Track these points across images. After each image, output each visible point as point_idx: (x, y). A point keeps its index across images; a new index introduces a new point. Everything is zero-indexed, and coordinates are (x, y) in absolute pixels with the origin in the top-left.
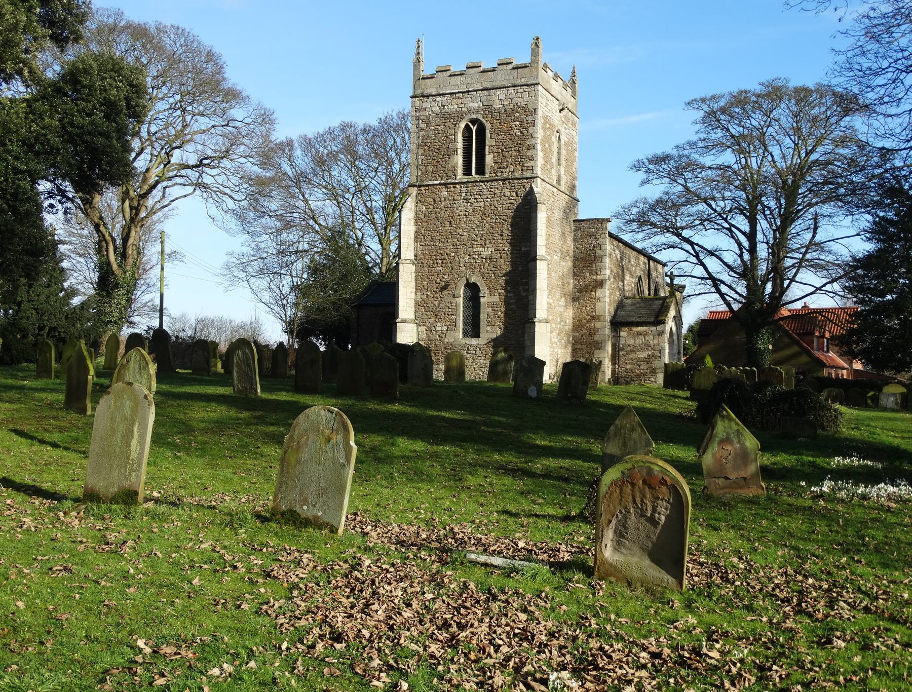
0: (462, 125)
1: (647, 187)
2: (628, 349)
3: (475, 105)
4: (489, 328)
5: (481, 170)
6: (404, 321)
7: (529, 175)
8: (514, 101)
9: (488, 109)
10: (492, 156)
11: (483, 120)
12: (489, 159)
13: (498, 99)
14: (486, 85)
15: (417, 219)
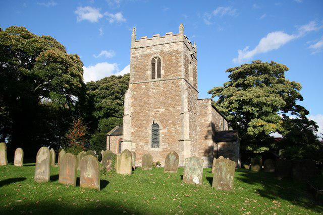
0: (151, 59)
3: (157, 51)
4: (164, 144)
5: (159, 76)
6: (126, 141)
9: (162, 53)
10: (164, 71)
11: (160, 57)
12: (162, 72)
13: (166, 48)
14: (161, 43)
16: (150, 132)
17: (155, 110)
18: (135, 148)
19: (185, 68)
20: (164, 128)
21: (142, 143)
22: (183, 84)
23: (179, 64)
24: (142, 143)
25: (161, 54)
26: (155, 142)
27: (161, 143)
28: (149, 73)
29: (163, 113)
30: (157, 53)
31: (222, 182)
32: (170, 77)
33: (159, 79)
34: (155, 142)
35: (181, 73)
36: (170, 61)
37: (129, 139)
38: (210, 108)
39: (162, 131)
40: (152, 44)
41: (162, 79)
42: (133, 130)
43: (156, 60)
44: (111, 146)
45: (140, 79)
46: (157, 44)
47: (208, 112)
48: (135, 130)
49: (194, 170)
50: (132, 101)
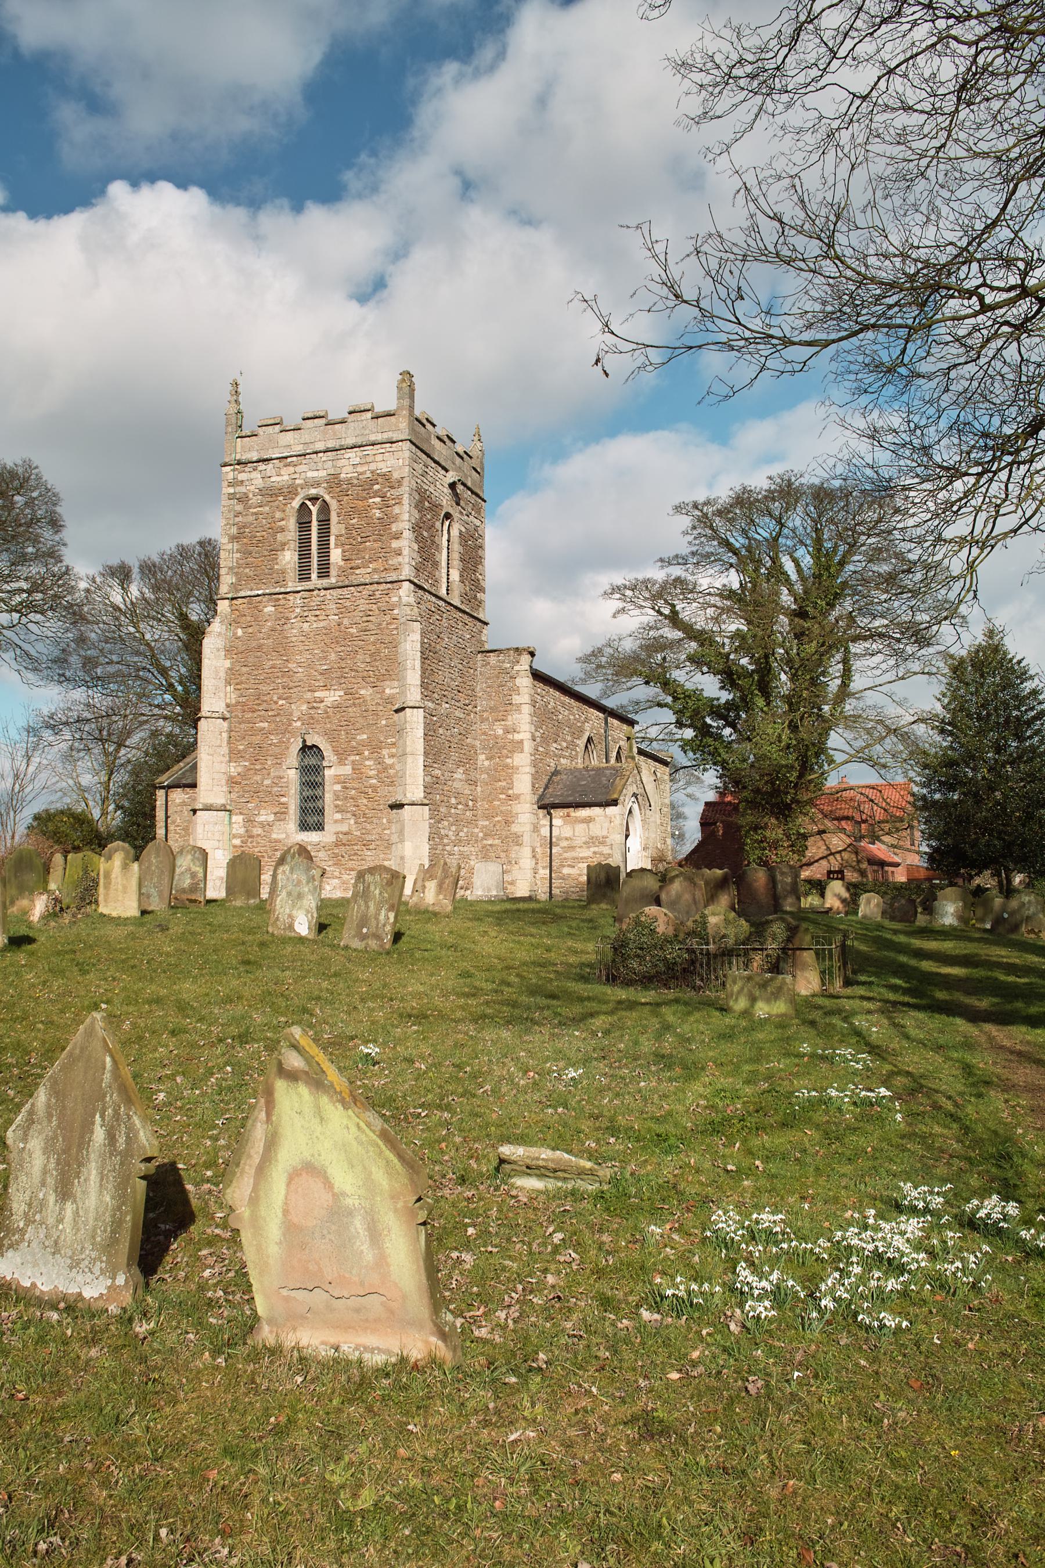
0: (296, 504)
1: (623, 618)
2: (564, 844)
3: (315, 474)
4: (338, 816)
5: (324, 573)
6: (207, 808)
7: (395, 578)
8: (373, 467)
9: (334, 482)
11: (327, 498)
12: (336, 555)
13: (349, 465)
15: (228, 651)
16: (293, 775)
17: (309, 695)
18: (242, 831)
19: (419, 539)
20: (341, 762)
21: (265, 816)
22: (405, 600)
23: (394, 528)
24: (265, 816)
25: (330, 489)
26: (311, 817)
27: (331, 816)
28: (289, 558)
29: (337, 707)
30: (317, 484)
31: (365, 930)
32: (363, 575)
33: (325, 582)
34: (311, 817)
35: (400, 559)
36: (364, 512)
37: (220, 800)
38: (525, 682)
39: (333, 772)
40: (299, 449)
41: (333, 580)
42: (234, 769)
43: (314, 509)
44: (171, 828)
45: (257, 579)
46: (320, 446)
47: (516, 699)
48: (240, 769)
49: (300, 896)
50: (228, 664)
